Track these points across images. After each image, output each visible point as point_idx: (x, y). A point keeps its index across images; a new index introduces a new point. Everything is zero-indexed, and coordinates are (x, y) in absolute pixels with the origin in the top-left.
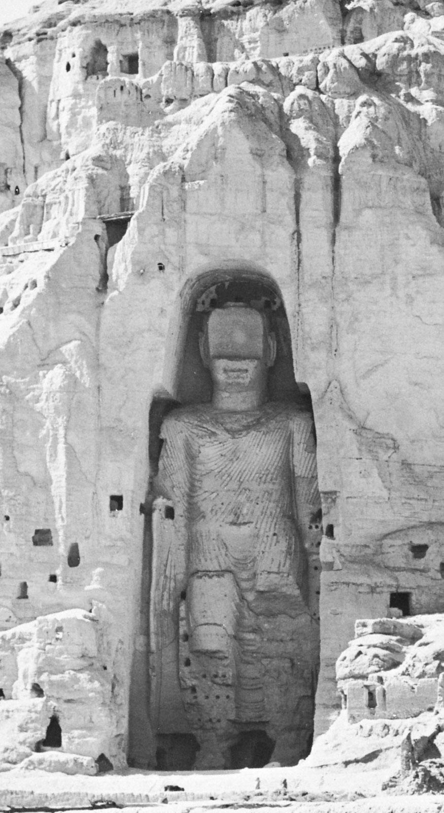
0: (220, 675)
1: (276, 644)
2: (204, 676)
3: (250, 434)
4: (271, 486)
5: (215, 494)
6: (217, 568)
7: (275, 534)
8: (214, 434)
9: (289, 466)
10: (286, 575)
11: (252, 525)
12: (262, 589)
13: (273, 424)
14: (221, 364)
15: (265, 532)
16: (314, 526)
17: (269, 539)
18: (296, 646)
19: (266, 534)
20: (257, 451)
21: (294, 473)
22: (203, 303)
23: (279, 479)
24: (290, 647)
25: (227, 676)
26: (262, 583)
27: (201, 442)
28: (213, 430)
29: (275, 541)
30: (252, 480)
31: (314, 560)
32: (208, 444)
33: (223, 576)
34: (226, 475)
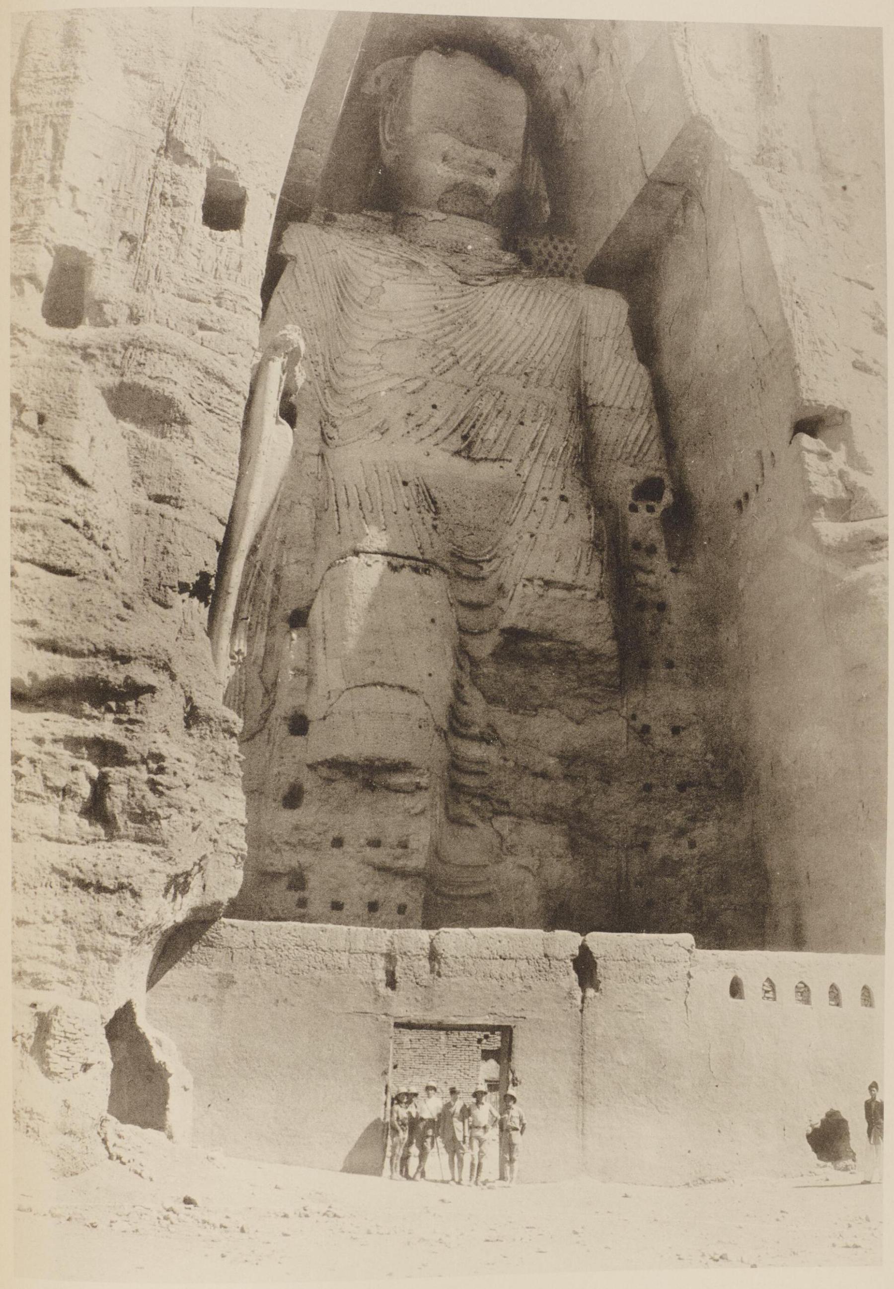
0: (392, 839)
2: (338, 843)
6: (416, 553)
7: (563, 498)
10: (590, 595)
11: (510, 467)
12: (522, 625)
15: (541, 488)
16: (641, 506)
17: (551, 504)
18: (581, 793)
19: (545, 493)
20: (522, 319)
21: (587, 399)
22: (378, 81)
25: (413, 844)
26: (512, 616)
29: (563, 515)
30: (509, 374)
33: (426, 571)
34: (447, 352)
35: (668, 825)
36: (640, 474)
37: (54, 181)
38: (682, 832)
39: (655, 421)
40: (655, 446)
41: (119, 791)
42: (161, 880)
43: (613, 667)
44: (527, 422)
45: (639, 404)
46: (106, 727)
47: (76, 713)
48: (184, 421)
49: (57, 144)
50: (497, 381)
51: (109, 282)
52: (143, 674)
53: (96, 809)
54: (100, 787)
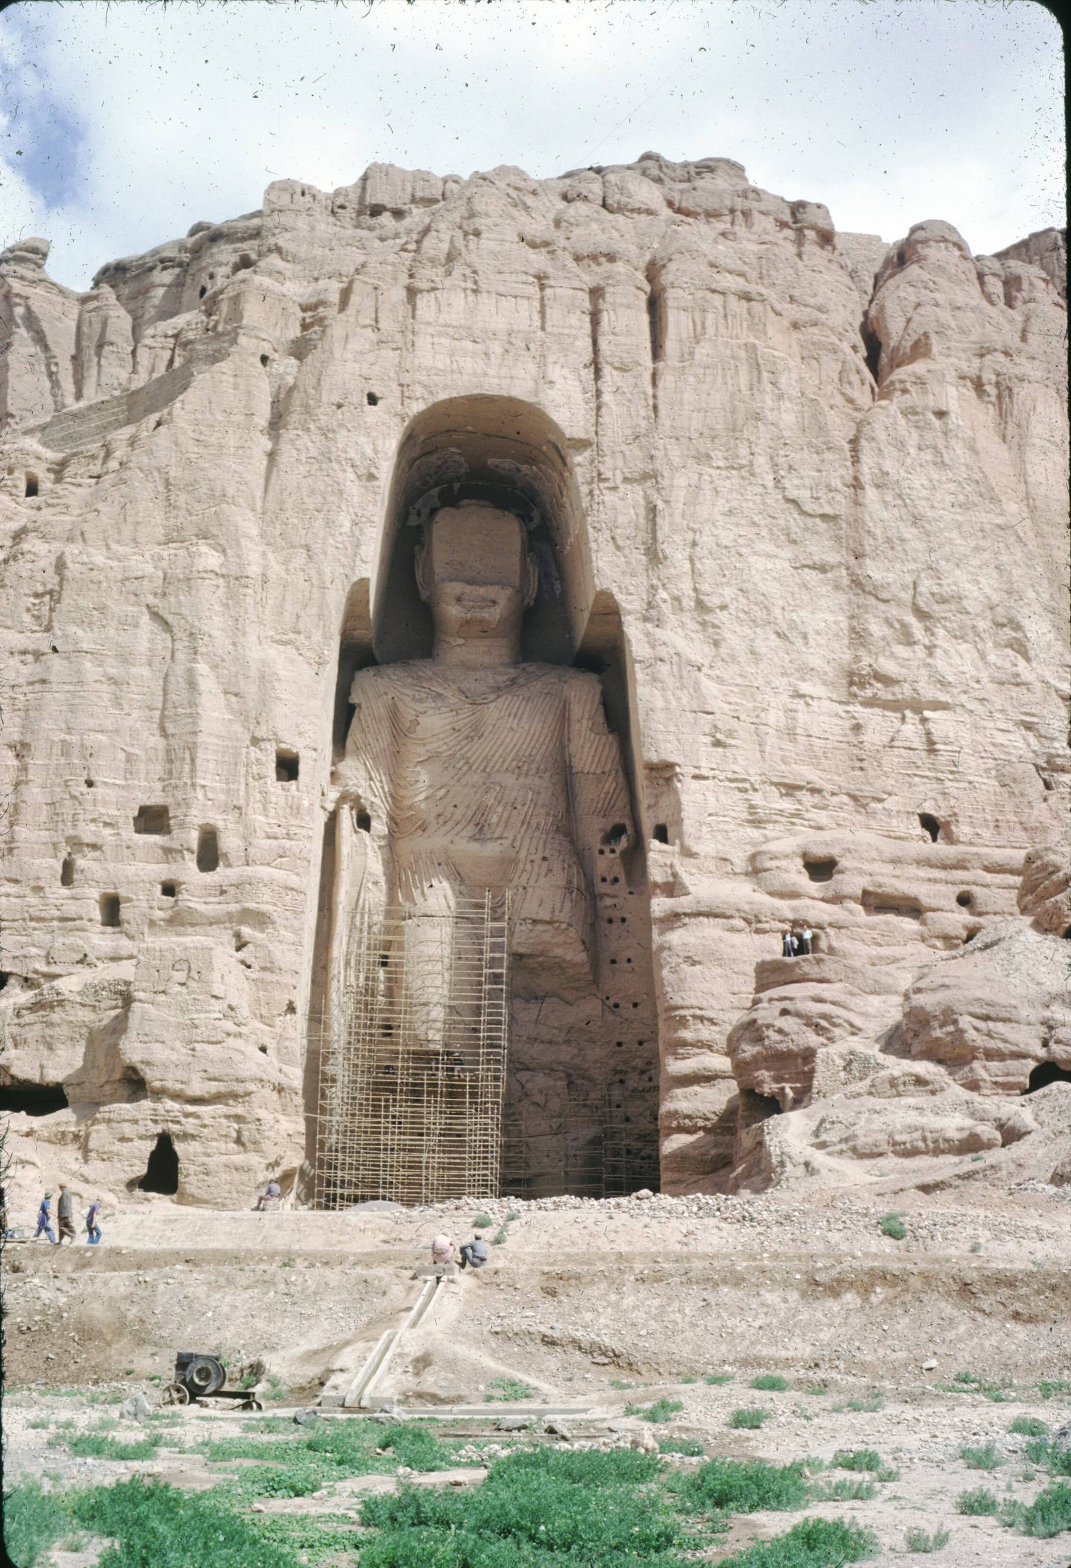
1: (541, 1047)
3: (502, 699)
4: (537, 782)
5: (442, 792)
8: (440, 695)
9: (563, 756)
13: (537, 686)
14: (455, 588)
23: (547, 775)
24: (566, 1053)
27: (420, 707)
28: (440, 690)
31: (606, 907)
32: (431, 712)
35: (634, 1068)
36: (608, 824)
37: (193, 785)
38: (643, 1072)
39: (621, 779)
40: (622, 795)
41: (246, 1134)
42: (263, 1166)
43: (586, 969)
44: (519, 807)
45: (607, 769)
46: (239, 1110)
47: (227, 1105)
48: (273, 923)
49: (193, 760)
50: (498, 778)
51: (229, 842)
52: (252, 1087)
53: (239, 1141)
54: (239, 1132)
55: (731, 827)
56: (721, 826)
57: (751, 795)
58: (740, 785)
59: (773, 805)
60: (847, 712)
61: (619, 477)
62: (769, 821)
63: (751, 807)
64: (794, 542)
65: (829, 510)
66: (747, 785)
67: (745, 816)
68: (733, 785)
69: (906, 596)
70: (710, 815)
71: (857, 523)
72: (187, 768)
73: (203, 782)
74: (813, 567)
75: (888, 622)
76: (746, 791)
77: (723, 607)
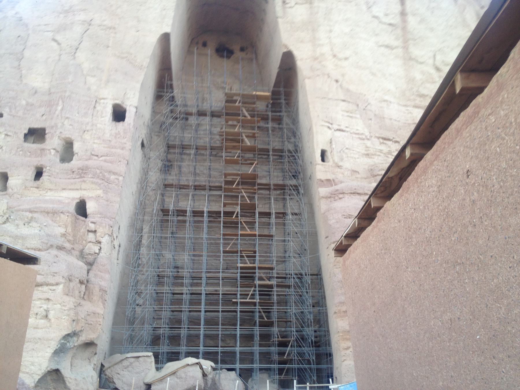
55: (357, 156)
56: (352, 155)
57: (366, 141)
58: (360, 136)
59: (377, 147)
60: (407, 110)
61: (292, 4)
62: (375, 155)
63: (367, 147)
64: (377, 35)
65: (392, 22)
66: (364, 137)
67: (363, 152)
68: (357, 136)
69: (431, 61)
70: (347, 149)
71: (404, 29)
72: (59, 108)
73: (68, 115)
74: (387, 46)
75: (423, 73)
76: (363, 139)
77: (346, 59)
